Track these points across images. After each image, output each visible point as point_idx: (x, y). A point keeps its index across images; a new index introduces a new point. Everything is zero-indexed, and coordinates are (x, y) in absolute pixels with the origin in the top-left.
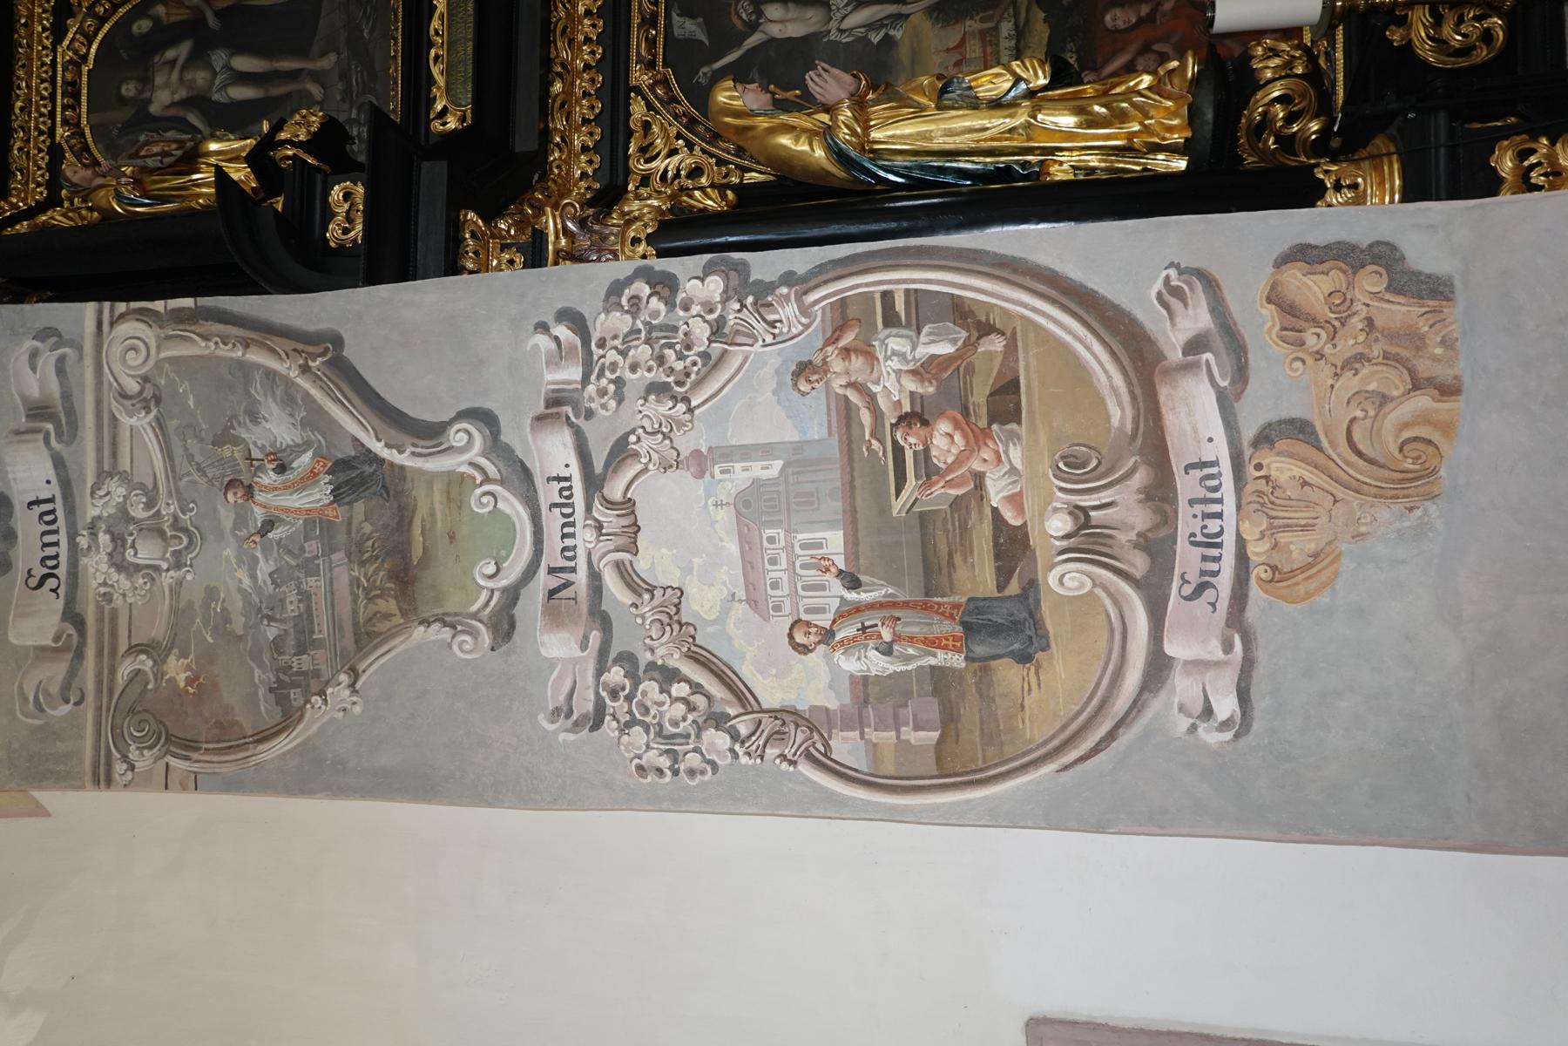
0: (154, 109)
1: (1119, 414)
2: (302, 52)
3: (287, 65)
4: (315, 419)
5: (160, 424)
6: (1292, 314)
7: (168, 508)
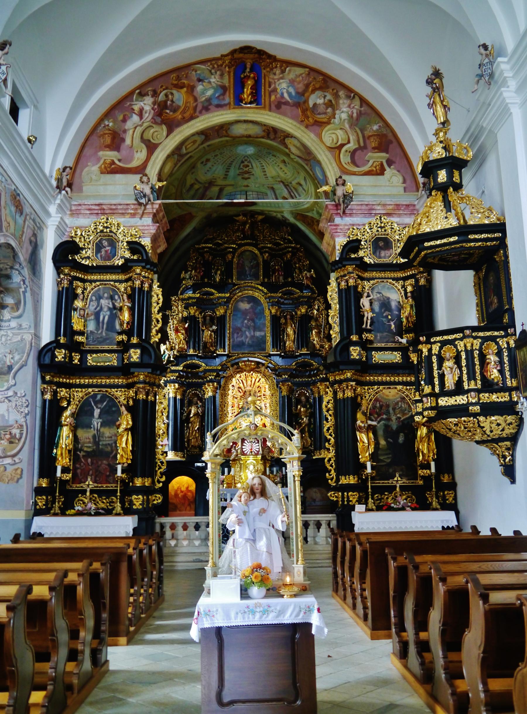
0: (101, 300)
1: (9, 454)
2: (107, 329)
3: (105, 326)
4: (17, 362)
5: (19, 341)
6: (16, 470)
7: (9, 342)
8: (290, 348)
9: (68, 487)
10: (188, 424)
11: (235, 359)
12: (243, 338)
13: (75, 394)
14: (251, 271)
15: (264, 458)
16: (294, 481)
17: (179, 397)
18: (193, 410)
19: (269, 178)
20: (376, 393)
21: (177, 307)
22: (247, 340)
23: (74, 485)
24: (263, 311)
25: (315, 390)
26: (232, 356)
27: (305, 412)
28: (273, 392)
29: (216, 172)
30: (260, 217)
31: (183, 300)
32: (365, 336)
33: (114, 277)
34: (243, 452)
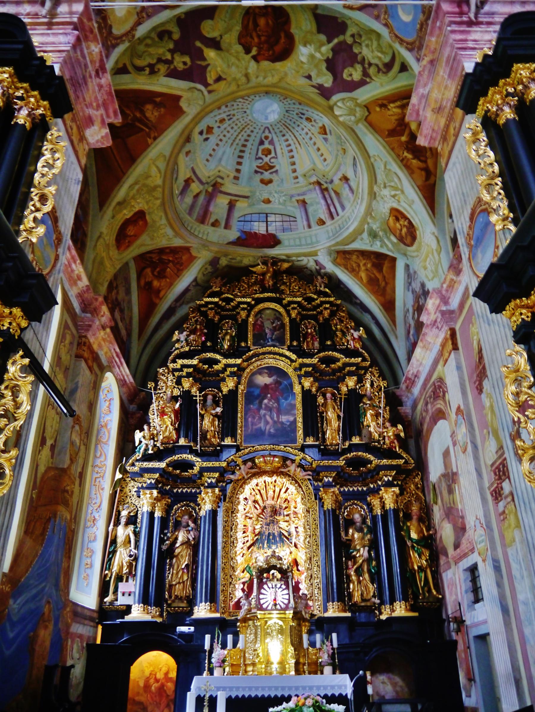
8: (332, 439)
10: (171, 559)
12: (262, 425)
14: (273, 334)
15: (297, 616)
18: (181, 536)
19: (301, 179)
21: (165, 382)
22: (268, 427)
24: (291, 386)
25: (376, 502)
27: (363, 538)
29: (223, 163)
30: (286, 265)
31: (175, 370)
34: (261, 605)
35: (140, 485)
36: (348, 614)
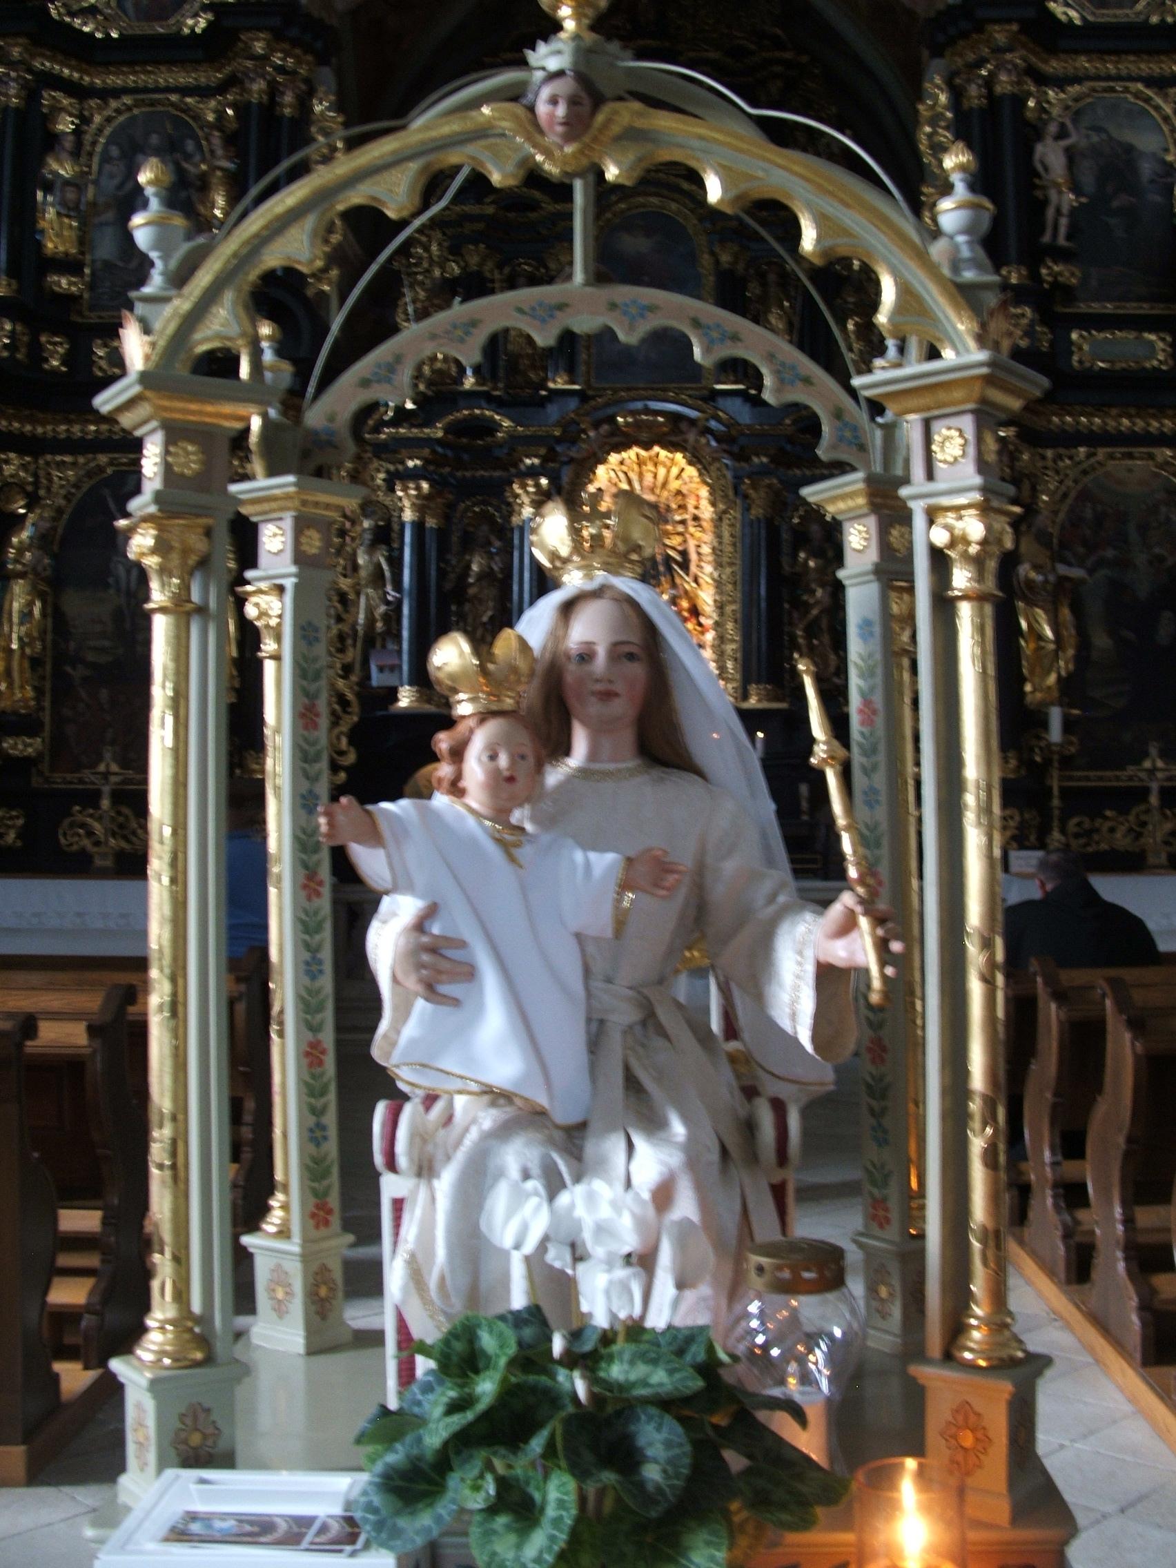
9: (36, 782)
10: (460, 604)
11: (607, 405)
13: (56, 473)
16: (944, 606)
17: (431, 523)
20: (1085, 472)
21: (427, 249)
23: (57, 777)
26: (593, 398)
28: (721, 506)
32: (1051, 270)
33: (184, 78)
35: (392, 468)
36: (783, 705)
